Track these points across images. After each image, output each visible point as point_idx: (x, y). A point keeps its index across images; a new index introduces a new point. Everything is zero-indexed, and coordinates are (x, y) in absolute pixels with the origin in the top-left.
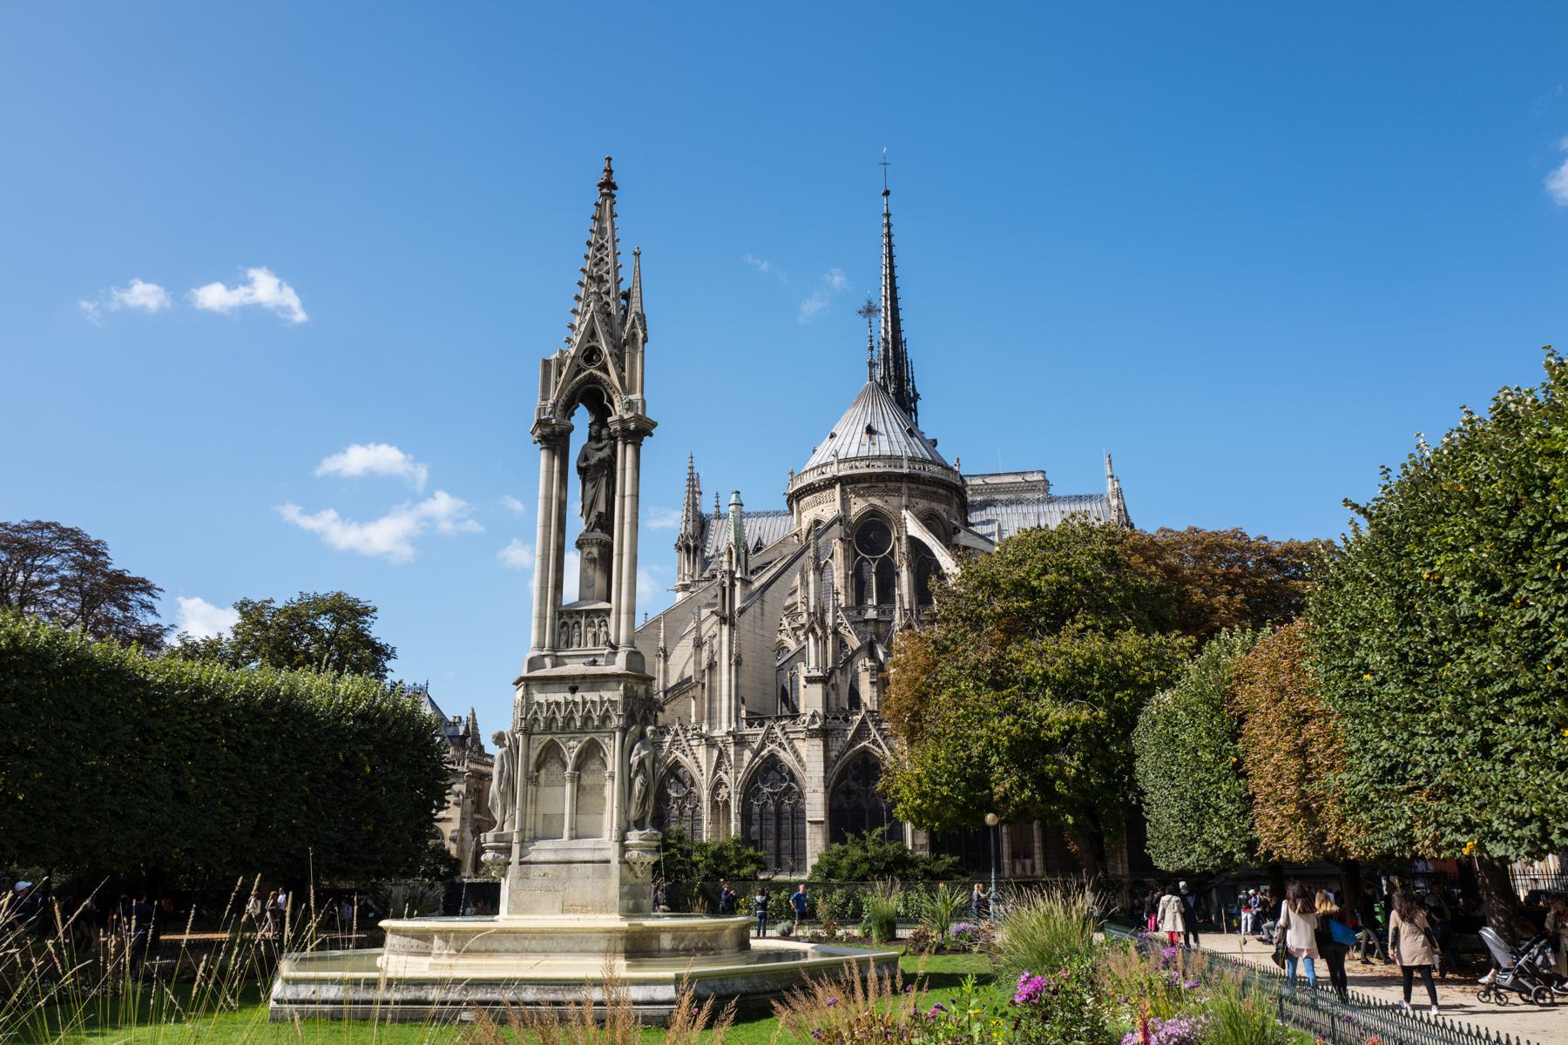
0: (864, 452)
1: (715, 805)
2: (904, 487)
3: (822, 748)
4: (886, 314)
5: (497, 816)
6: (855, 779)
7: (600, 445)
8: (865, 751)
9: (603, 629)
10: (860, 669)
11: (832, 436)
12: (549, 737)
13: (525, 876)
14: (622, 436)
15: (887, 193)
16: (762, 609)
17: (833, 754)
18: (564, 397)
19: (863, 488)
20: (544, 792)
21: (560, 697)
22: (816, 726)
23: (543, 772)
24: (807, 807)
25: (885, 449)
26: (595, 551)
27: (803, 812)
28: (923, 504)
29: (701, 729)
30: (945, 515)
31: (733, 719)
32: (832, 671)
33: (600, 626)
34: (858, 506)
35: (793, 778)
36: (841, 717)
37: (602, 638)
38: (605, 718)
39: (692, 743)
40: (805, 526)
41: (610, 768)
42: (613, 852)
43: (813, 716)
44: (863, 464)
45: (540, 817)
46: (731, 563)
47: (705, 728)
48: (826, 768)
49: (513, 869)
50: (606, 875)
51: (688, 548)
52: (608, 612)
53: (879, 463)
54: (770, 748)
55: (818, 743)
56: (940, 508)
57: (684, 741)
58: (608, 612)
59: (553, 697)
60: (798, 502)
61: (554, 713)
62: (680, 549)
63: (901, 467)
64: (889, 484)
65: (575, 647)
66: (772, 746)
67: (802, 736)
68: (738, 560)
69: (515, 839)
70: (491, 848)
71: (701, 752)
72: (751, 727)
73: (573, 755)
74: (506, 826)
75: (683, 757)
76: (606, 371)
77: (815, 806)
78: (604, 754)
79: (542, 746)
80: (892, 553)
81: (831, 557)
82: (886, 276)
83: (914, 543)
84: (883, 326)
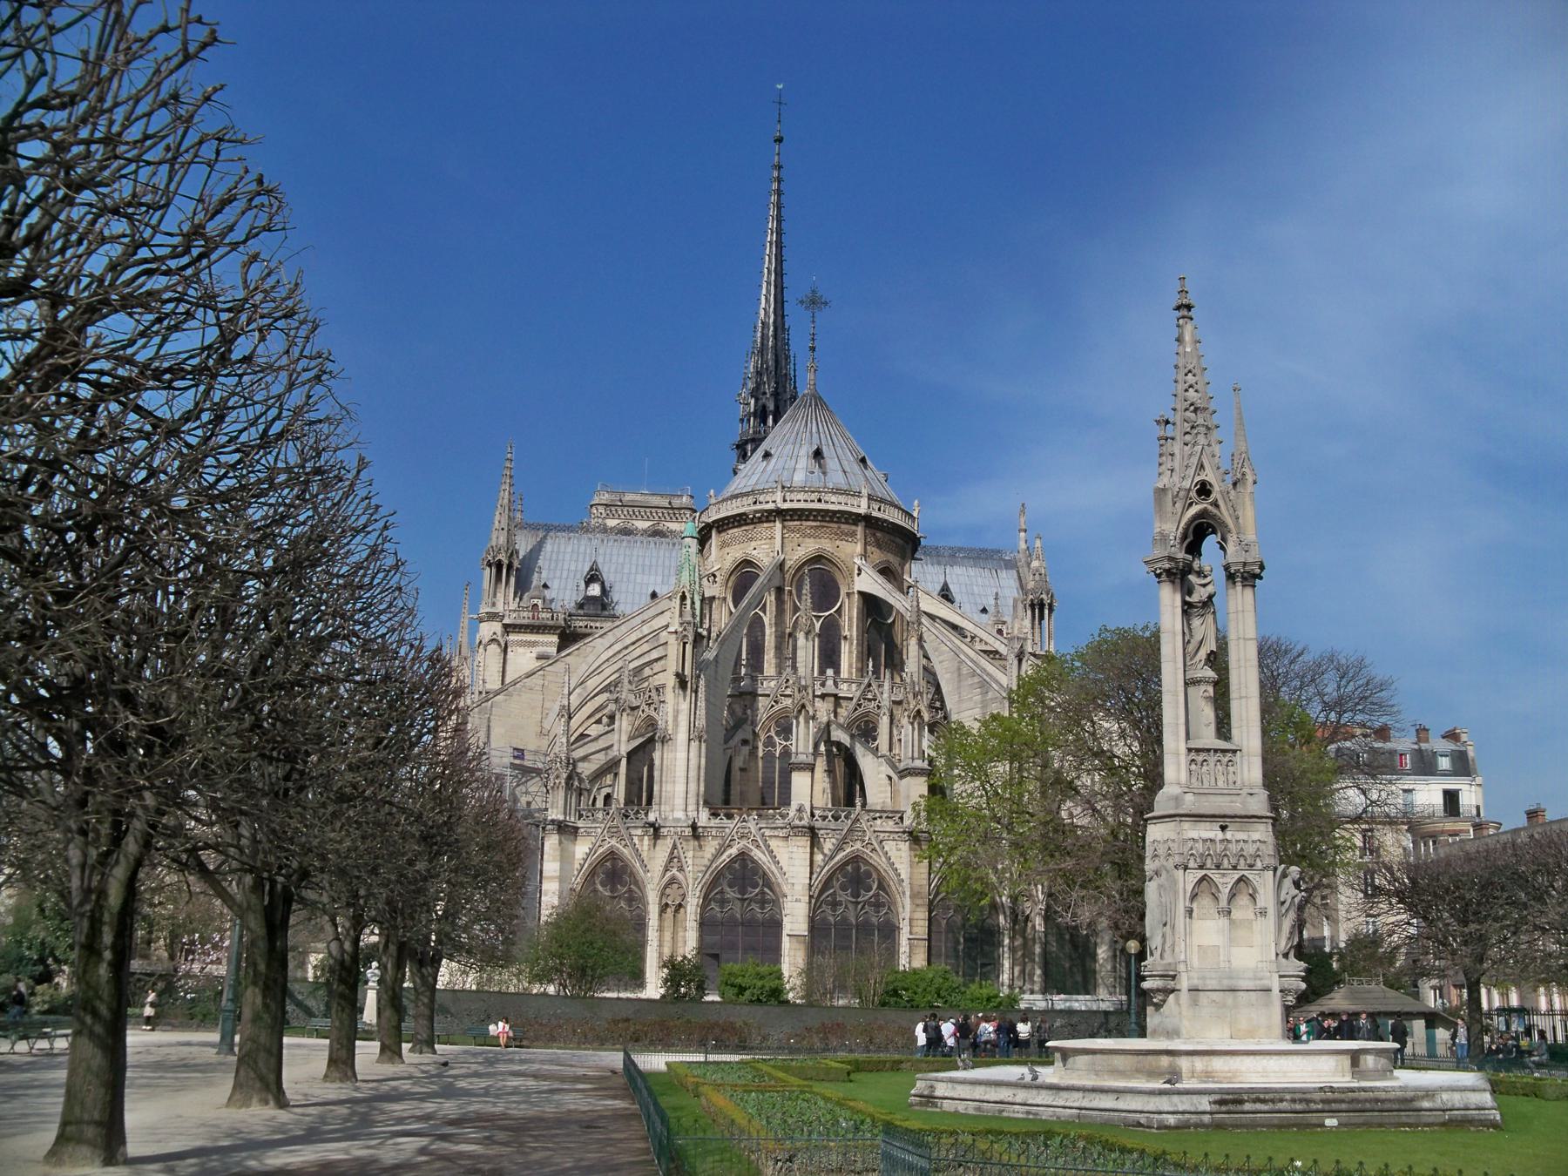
0: (816, 480)
1: (664, 908)
2: (860, 529)
3: (808, 850)
4: (768, 291)
6: (843, 888)
7: (1203, 582)
8: (856, 859)
9: (1231, 769)
11: (767, 455)
13: (1195, 1003)
14: (1243, 577)
15: (779, 140)
16: (716, 672)
17: (819, 858)
18: (1180, 529)
20: (1197, 924)
22: (803, 823)
23: (1195, 906)
24: (785, 920)
25: (836, 478)
26: (1211, 689)
27: (775, 925)
28: (878, 556)
31: (692, 807)
34: (803, 548)
35: (768, 883)
37: (1231, 777)
39: (633, 832)
41: (1261, 903)
42: (1276, 985)
43: (800, 810)
44: (815, 496)
45: (1195, 949)
48: (811, 873)
49: (1184, 996)
50: (1267, 1004)
51: (499, 565)
52: (1234, 752)
53: (833, 498)
55: (805, 842)
56: (894, 560)
59: (1211, 835)
60: (719, 532)
61: (1209, 849)
62: (490, 565)
64: (843, 526)
65: (1206, 785)
66: (744, 842)
67: (781, 833)
73: (1227, 890)
74: (1165, 955)
76: (1216, 504)
77: (795, 918)
78: (1255, 890)
80: (839, 611)
81: (764, 609)
82: (771, 243)
84: (763, 305)
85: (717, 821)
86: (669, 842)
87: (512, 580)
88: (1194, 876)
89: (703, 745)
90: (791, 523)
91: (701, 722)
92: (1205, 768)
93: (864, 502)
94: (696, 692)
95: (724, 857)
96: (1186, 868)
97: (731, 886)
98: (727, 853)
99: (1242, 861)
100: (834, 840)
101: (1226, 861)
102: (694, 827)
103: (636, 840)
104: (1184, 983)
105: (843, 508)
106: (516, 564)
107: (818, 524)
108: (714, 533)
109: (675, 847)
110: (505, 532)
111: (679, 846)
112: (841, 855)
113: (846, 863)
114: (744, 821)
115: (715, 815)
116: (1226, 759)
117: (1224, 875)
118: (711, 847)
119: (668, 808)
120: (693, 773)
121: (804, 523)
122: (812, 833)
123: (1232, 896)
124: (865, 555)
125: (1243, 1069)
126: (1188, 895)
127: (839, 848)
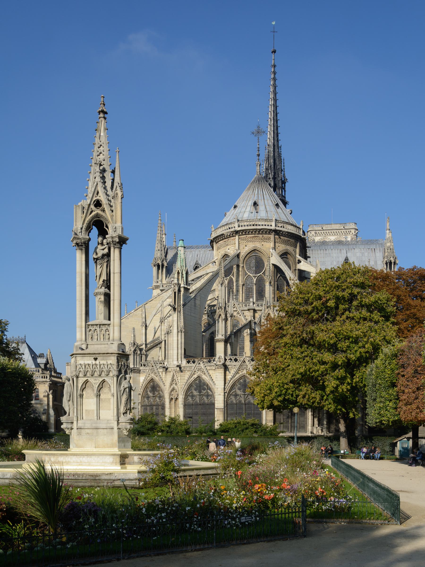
2: (272, 236)
5: (67, 409)
9: (107, 333)
10: (245, 335)
12: (86, 379)
16: (195, 303)
19: (251, 237)
21: (90, 362)
23: (84, 393)
28: (282, 247)
29: (164, 364)
30: (293, 253)
31: (179, 359)
32: (230, 336)
33: (106, 331)
35: (210, 389)
36: (233, 359)
37: (107, 337)
38: (109, 372)
40: (220, 257)
41: (112, 392)
46: (178, 279)
47: (166, 363)
49: (74, 431)
51: (158, 266)
52: (109, 325)
54: (198, 374)
55: (222, 371)
56: (290, 249)
57: (155, 369)
58: (109, 325)
59: (87, 362)
61: (88, 369)
62: (155, 266)
63: (271, 226)
64: (264, 235)
68: (182, 277)
69: (75, 419)
70: (65, 422)
71: (163, 375)
72: (188, 363)
73: (97, 386)
75: (155, 377)
79: (83, 382)
83: (275, 266)
85: (190, 364)
86: (172, 374)
87: (164, 269)
88: (81, 380)
89: (183, 334)
90: (242, 236)
91: (182, 324)
92: (96, 333)
93: (273, 224)
94: (180, 312)
95: (192, 378)
96: (77, 377)
97: (195, 390)
98: (193, 377)
99: (103, 373)
100: (234, 370)
101: (96, 373)
102: (179, 367)
103: (160, 374)
104: (75, 426)
105: (264, 227)
106: (165, 264)
107: (253, 235)
108: (214, 243)
109: (174, 376)
110: (160, 251)
111: (175, 375)
112: (238, 376)
113: (240, 378)
114: (199, 364)
115: (188, 362)
116: (106, 328)
117: (95, 379)
118: (187, 375)
119: (171, 360)
120: (179, 346)
121: (248, 236)
122: (226, 368)
123: (100, 389)
124: (274, 248)
125: (72, 461)
126: (79, 388)
127: (237, 373)
